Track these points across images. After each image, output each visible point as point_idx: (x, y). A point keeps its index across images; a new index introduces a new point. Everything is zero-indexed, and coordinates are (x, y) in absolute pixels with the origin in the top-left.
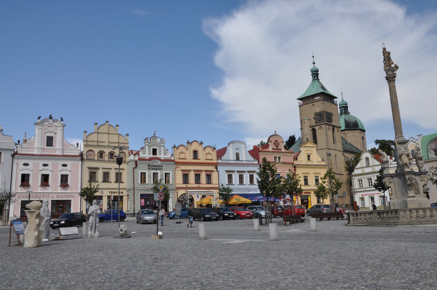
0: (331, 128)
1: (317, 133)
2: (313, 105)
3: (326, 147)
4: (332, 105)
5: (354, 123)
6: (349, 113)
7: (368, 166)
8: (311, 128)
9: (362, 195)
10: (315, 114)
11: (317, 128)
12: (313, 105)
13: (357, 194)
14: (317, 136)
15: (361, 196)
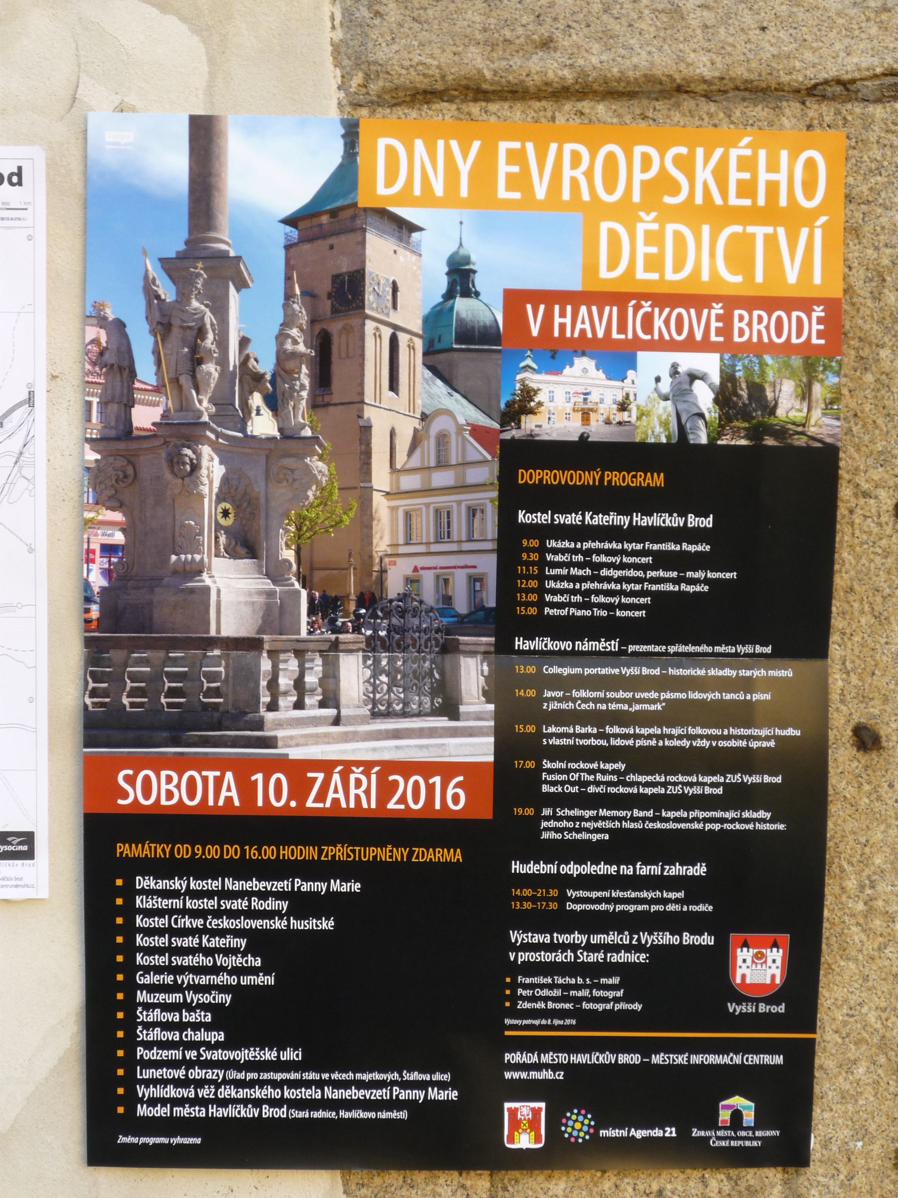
0: (387, 332)
1: (335, 349)
2: (332, 247)
3: (357, 399)
4: (401, 251)
5: (485, 327)
6: (477, 294)
7: (442, 464)
8: (318, 328)
9: (416, 570)
10: (336, 278)
11: (335, 328)
12: (332, 247)
13: (399, 561)
14: (334, 358)
15: (409, 572)
